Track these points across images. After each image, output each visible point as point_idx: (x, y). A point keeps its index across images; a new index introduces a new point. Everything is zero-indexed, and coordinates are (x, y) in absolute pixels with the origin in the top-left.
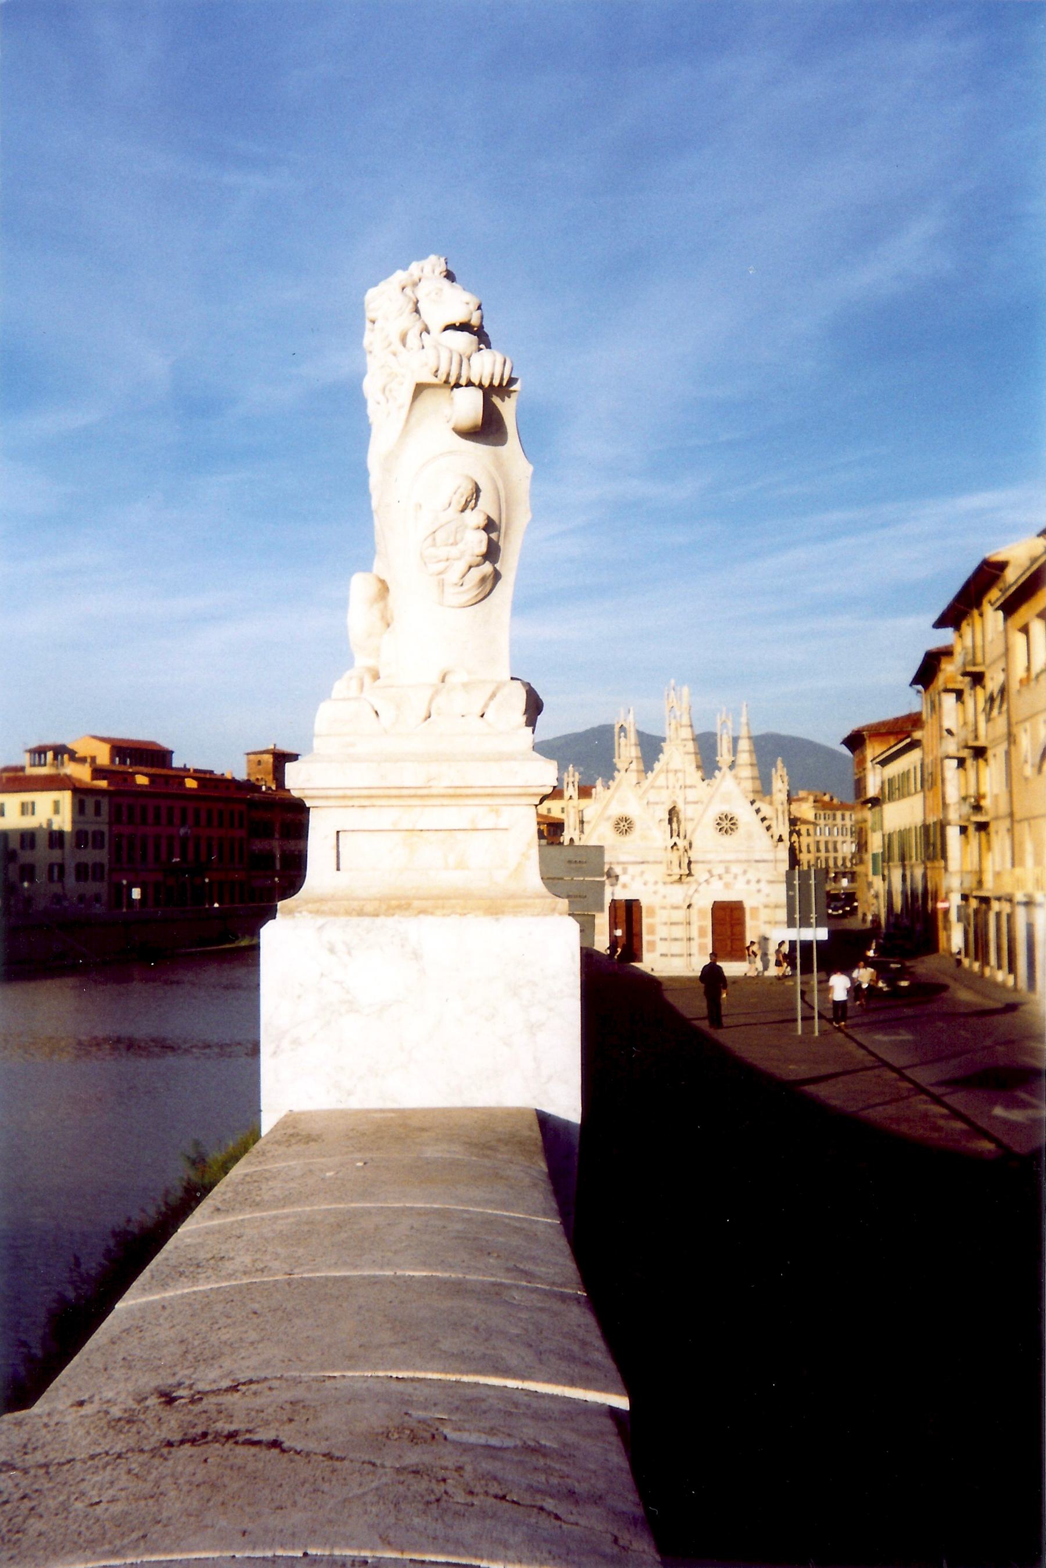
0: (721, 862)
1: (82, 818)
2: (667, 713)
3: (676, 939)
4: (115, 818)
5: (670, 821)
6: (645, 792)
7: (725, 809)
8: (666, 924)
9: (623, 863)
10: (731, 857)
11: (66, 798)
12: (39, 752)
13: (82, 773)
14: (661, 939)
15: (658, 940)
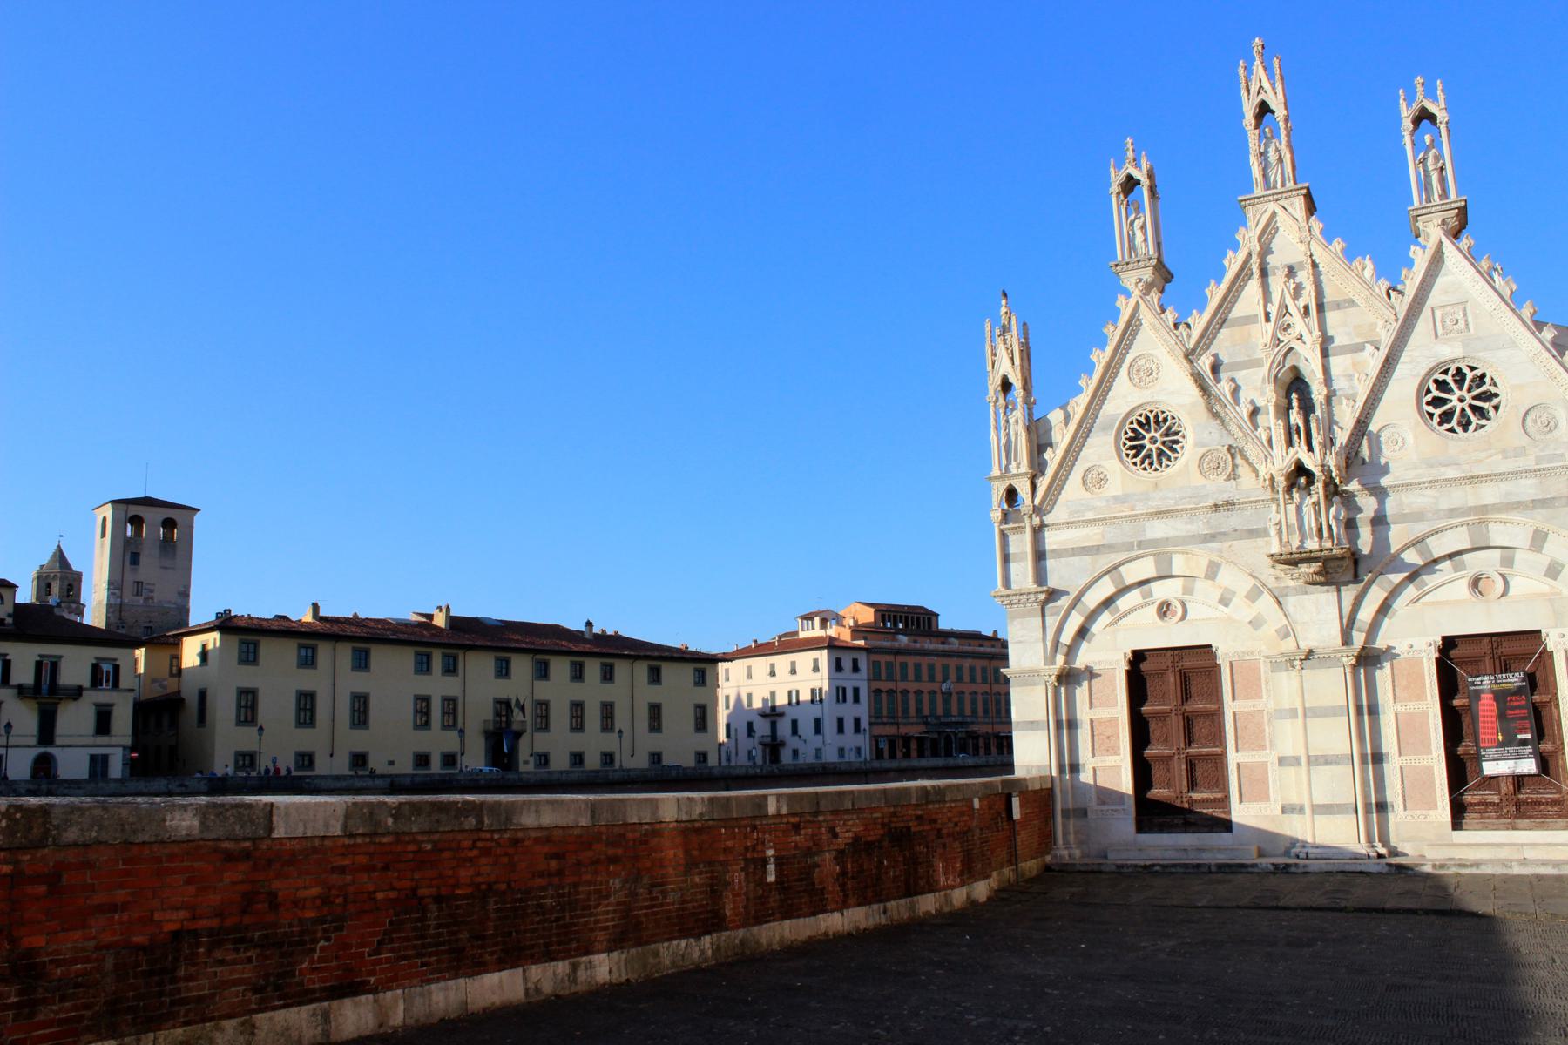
0: (1452, 512)
1: (839, 675)
2: (1249, 119)
3: (1327, 761)
4: (875, 676)
5: (1284, 411)
6: (1208, 336)
7: (1449, 351)
8: (1293, 713)
9: (1155, 543)
10: (1490, 494)
11: (823, 656)
12: (809, 617)
13: (845, 635)
14: (1282, 761)
15: (1274, 772)
